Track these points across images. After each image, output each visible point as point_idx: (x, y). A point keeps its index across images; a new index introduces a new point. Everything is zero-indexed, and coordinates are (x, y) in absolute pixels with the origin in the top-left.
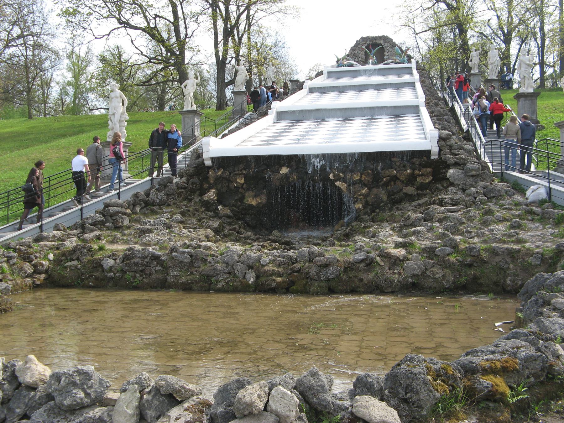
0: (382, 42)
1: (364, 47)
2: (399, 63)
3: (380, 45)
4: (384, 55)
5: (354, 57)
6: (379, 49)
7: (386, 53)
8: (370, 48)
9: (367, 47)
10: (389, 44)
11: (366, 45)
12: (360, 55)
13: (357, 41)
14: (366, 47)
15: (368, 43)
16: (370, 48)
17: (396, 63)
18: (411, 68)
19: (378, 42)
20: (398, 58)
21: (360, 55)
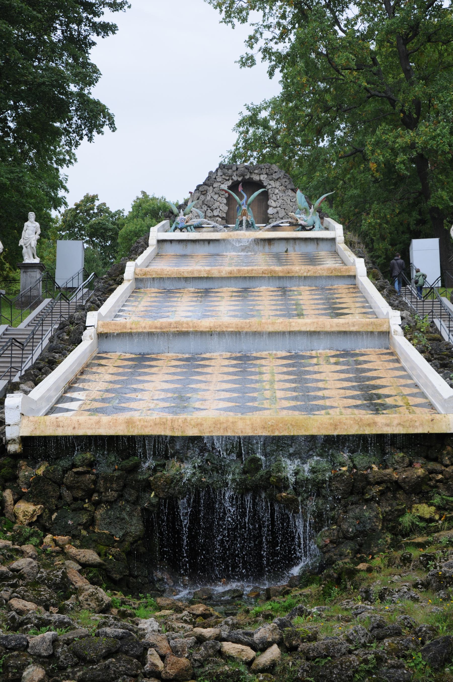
0: (263, 177)
1: (225, 187)
2: (304, 228)
3: (260, 185)
4: (268, 207)
5: (205, 208)
6: (259, 195)
7: (271, 202)
8: (240, 189)
9: (234, 187)
10: (278, 184)
11: (230, 183)
12: (217, 204)
13: (211, 173)
14: (230, 188)
15: (235, 178)
16: (240, 189)
17: (295, 225)
18: (333, 240)
19: (256, 178)
20: (303, 216)
21: (217, 204)
